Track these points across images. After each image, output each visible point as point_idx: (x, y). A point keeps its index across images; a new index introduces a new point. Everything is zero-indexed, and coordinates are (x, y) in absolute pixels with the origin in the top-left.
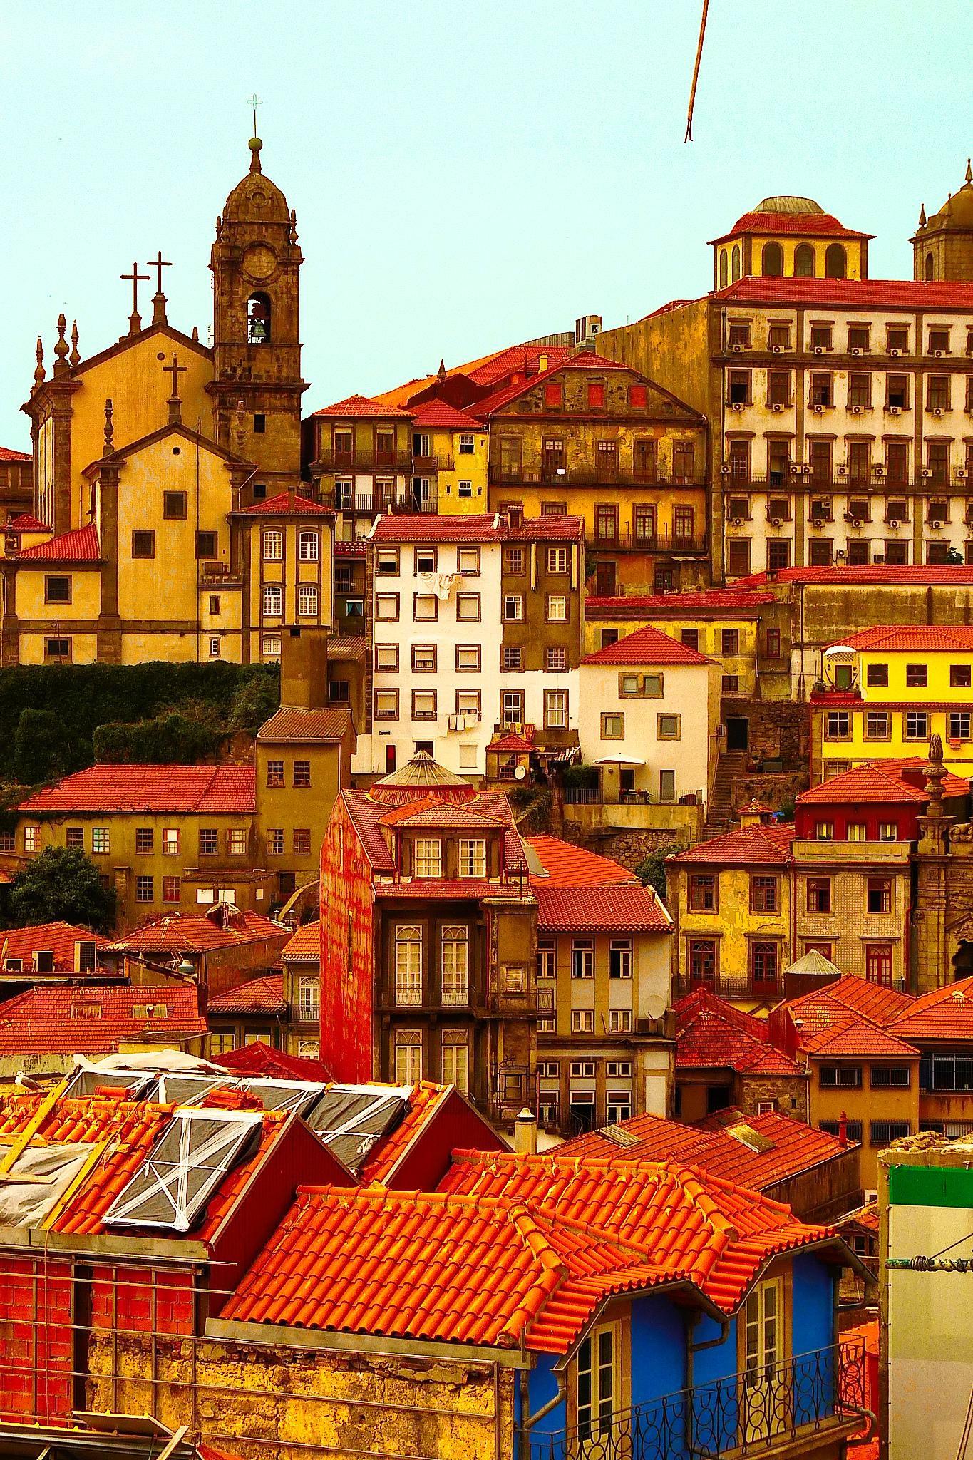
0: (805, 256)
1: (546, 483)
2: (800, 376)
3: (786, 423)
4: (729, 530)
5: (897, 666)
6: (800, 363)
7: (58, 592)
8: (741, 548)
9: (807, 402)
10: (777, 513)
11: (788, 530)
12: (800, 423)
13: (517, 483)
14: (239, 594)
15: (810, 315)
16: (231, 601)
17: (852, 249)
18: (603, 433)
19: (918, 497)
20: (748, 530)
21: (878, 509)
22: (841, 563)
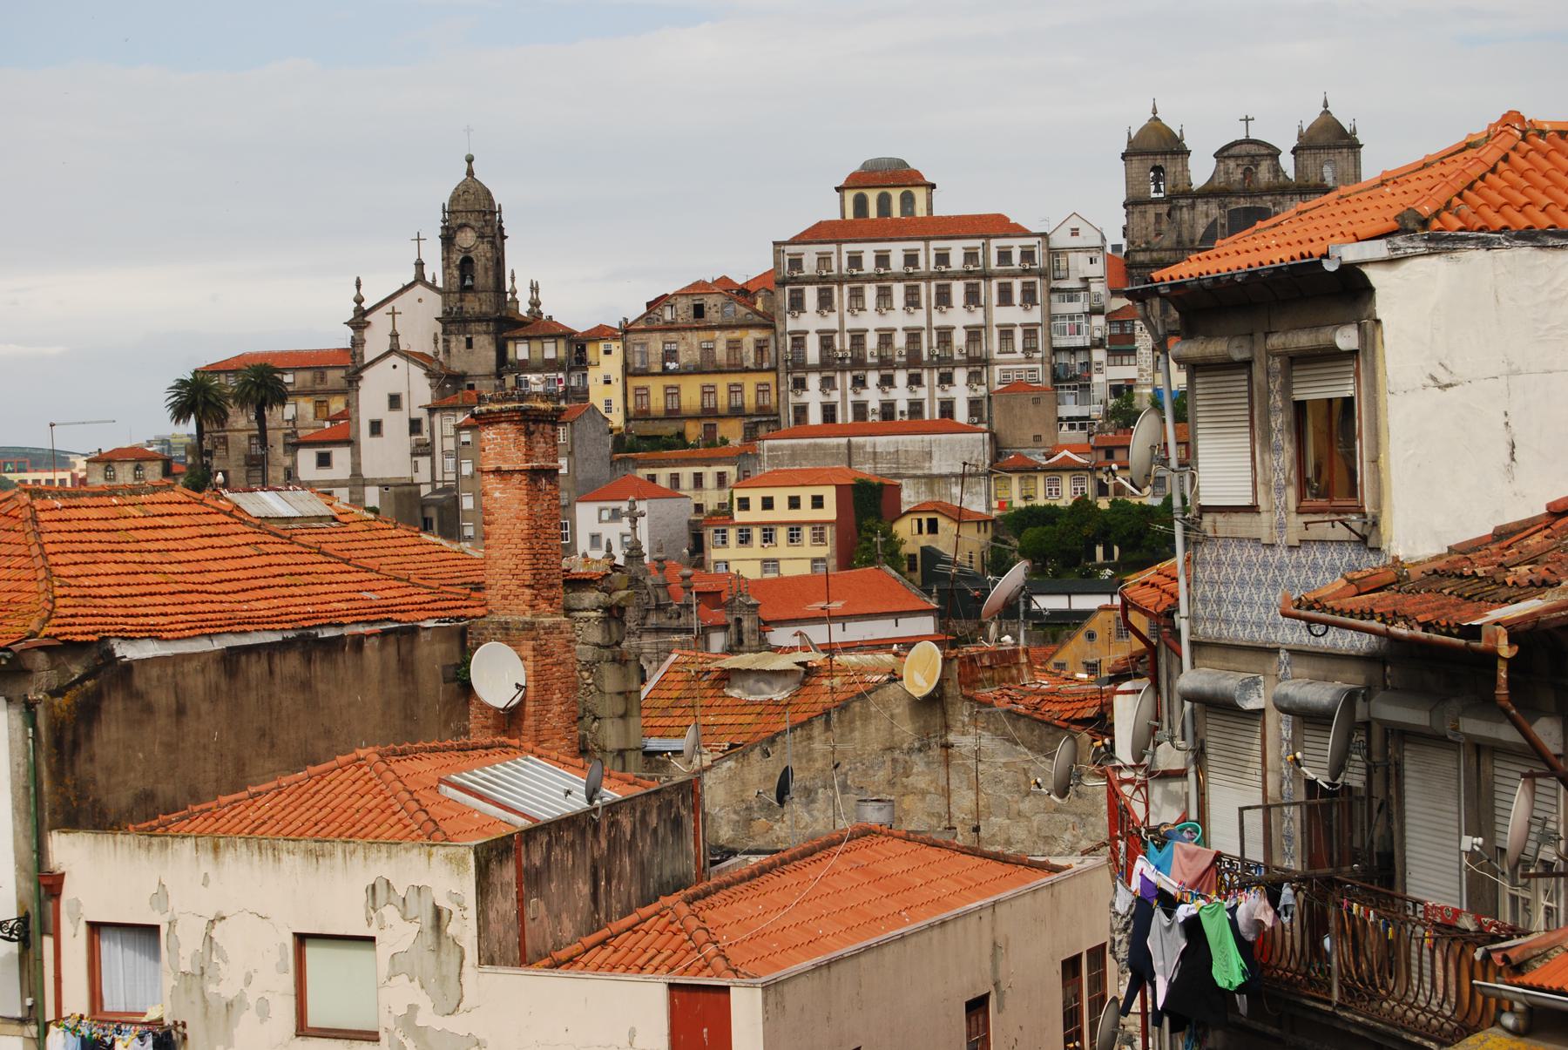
1: (666, 372)
2: (840, 290)
3: (831, 322)
4: (792, 399)
6: (840, 281)
7: (324, 461)
8: (801, 411)
9: (846, 306)
10: (828, 384)
11: (835, 396)
12: (842, 322)
13: (645, 373)
14: (428, 459)
15: (846, 247)
16: (424, 462)
17: (920, 194)
18: (703, 335)
19: (931, 368)
20: (806, 397)
21: (901, 377)
22: (877, 418)
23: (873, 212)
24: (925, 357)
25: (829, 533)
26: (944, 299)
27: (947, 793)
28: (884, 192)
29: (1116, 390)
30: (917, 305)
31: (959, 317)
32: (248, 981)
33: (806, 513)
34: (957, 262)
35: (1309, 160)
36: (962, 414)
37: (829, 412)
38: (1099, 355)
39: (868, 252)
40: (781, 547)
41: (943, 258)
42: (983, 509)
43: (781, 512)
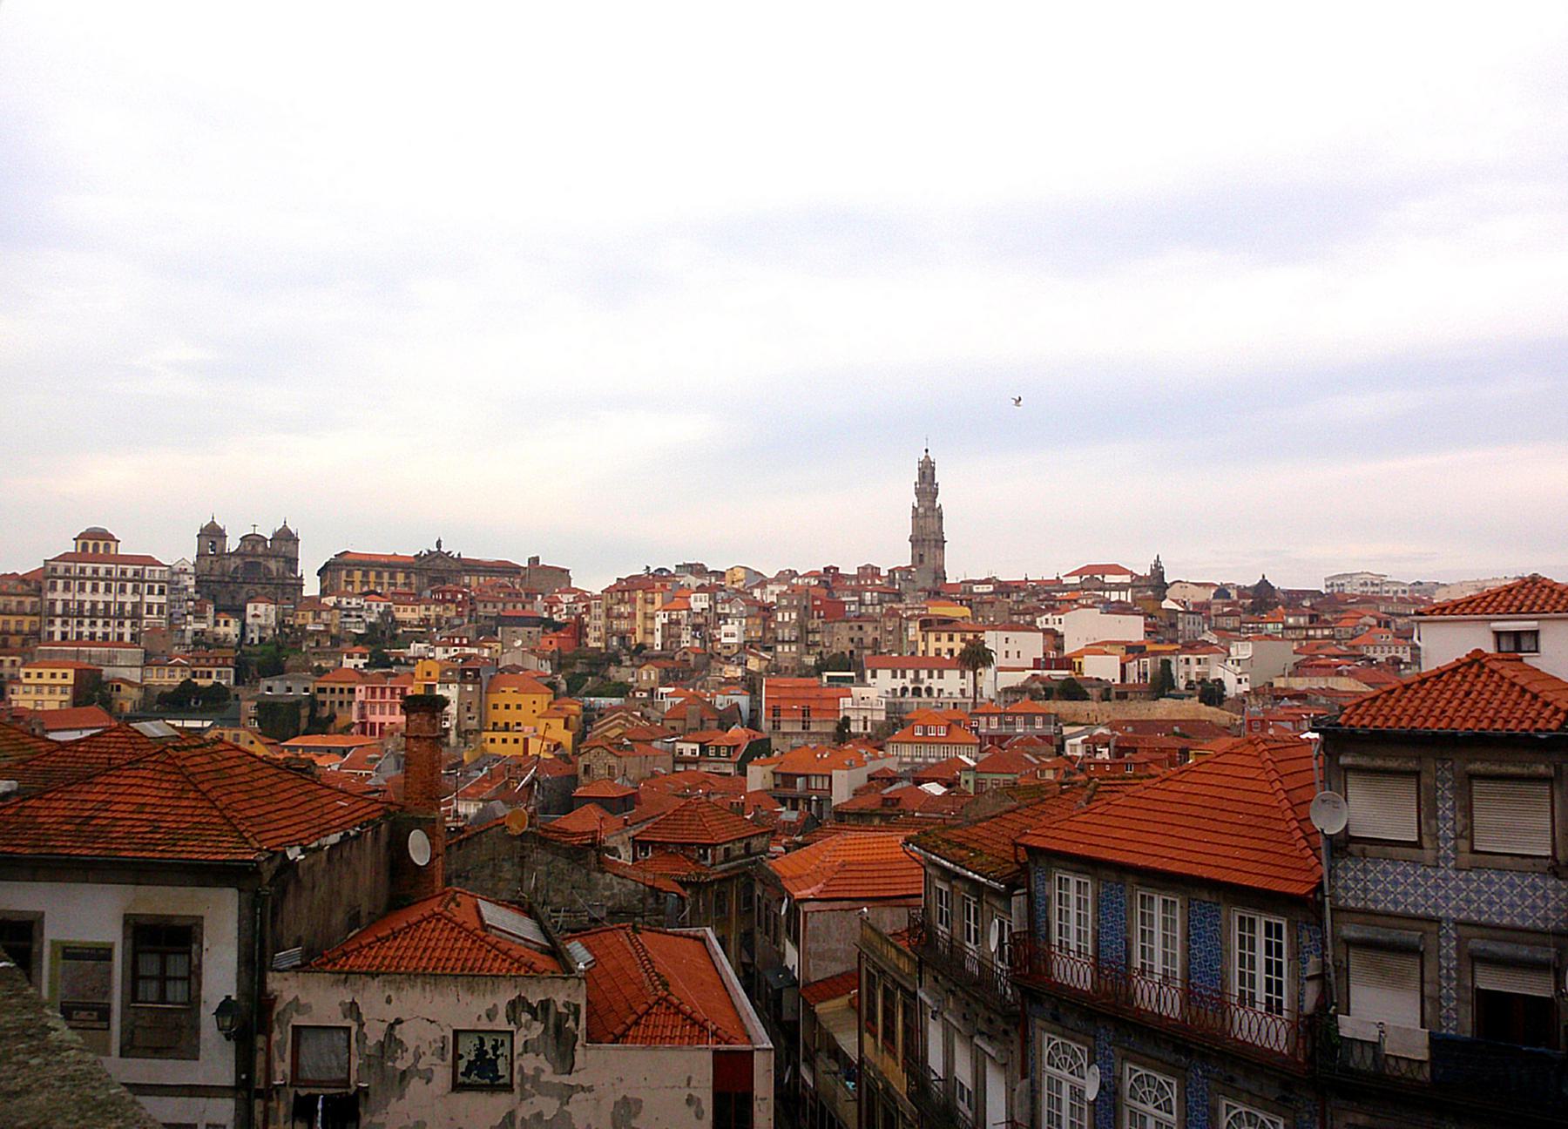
0: (96, 546)
3: (69, 596)
5: (34, 675)
6: (75, 579)
8: (51, 634)
10: (65, 623)
17: (113, 544)
21: (100, 622)
25: (69, 690)
26: (123, 590)
27: (521, 881)
28: (96, 542)
29: (196, 633)
31: (129, 598)
32: (418, 1057)
33: (59, 680)
34: (130, 574)
35: (277, 544)
36: (127, 638)
37: (64, 636)
38: (190, 618)
39: (89, 568)
40: (46, 696)
41: (124, 572)
43: (46, 679)
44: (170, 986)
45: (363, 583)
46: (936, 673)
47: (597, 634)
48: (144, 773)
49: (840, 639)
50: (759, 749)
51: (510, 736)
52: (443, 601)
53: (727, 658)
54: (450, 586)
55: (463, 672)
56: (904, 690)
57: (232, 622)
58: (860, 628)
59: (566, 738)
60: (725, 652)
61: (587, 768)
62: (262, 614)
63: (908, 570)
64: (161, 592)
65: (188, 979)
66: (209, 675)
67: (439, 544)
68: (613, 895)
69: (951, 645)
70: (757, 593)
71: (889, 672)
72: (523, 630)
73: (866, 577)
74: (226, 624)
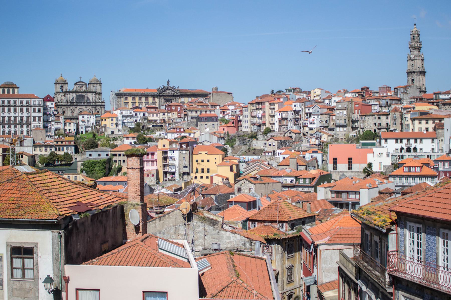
17: (16, 90)
23: (6, 93)
24: (18, 122)
26: (22, 110)
29: (56, 130)
30: (16, 112)
31: (25, 114)
38: (53, 123)
41: (22, 102)
42: (31, 153)
44: (26, 271)
45: (134, 103)
46: (418, 141)
47: (246, 125)
48: (13, 185)
49: (369, 124)
50: (325, 178)
51: (205, 175)
52: (171, 111)
53: (311, 135)
54: (174, 103)
55: (181, 146)
56: (402, 149)
57: (72, 124)
58: (379, 118)
59: (231, 176)
60: (310, 132)
61: (239, 190)
62: (88, 120)
63: (405, 88)
64: (39, 111)
65: (33, 269)
66: (63, 150)
67: (168, 83)
68: (231, 242)
69: (427, 126)
70: (327, 101)
71: (394, 141)
72: (210, 124)
73: (383, 92)
74: (70, 124)
